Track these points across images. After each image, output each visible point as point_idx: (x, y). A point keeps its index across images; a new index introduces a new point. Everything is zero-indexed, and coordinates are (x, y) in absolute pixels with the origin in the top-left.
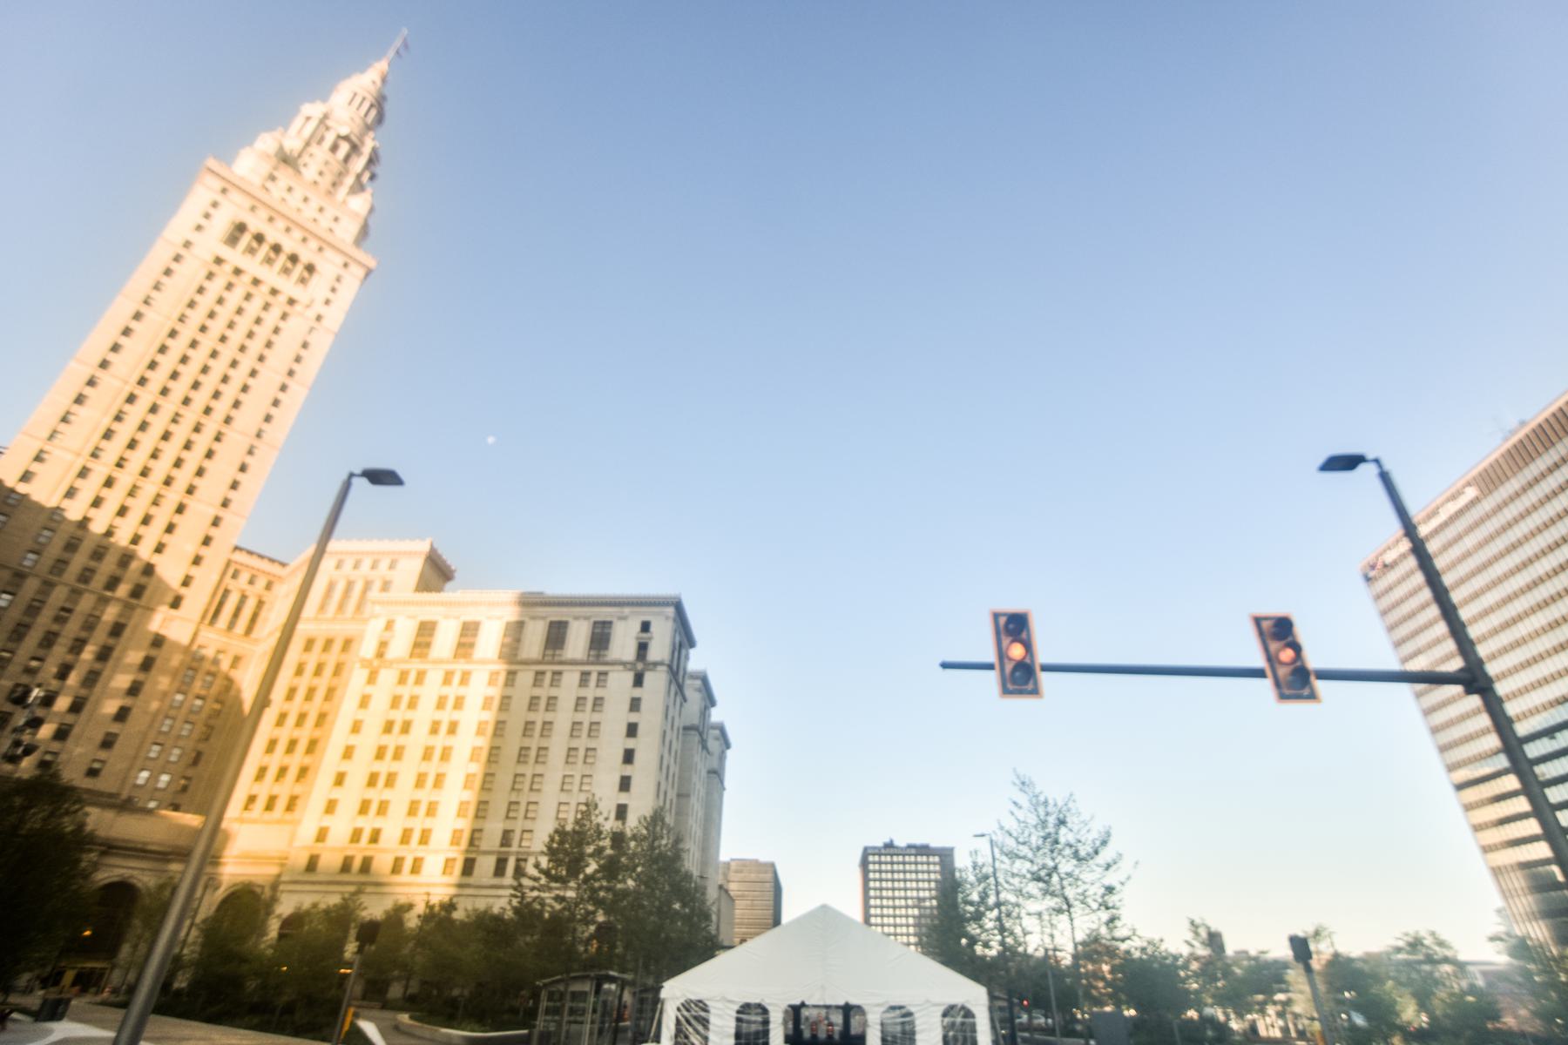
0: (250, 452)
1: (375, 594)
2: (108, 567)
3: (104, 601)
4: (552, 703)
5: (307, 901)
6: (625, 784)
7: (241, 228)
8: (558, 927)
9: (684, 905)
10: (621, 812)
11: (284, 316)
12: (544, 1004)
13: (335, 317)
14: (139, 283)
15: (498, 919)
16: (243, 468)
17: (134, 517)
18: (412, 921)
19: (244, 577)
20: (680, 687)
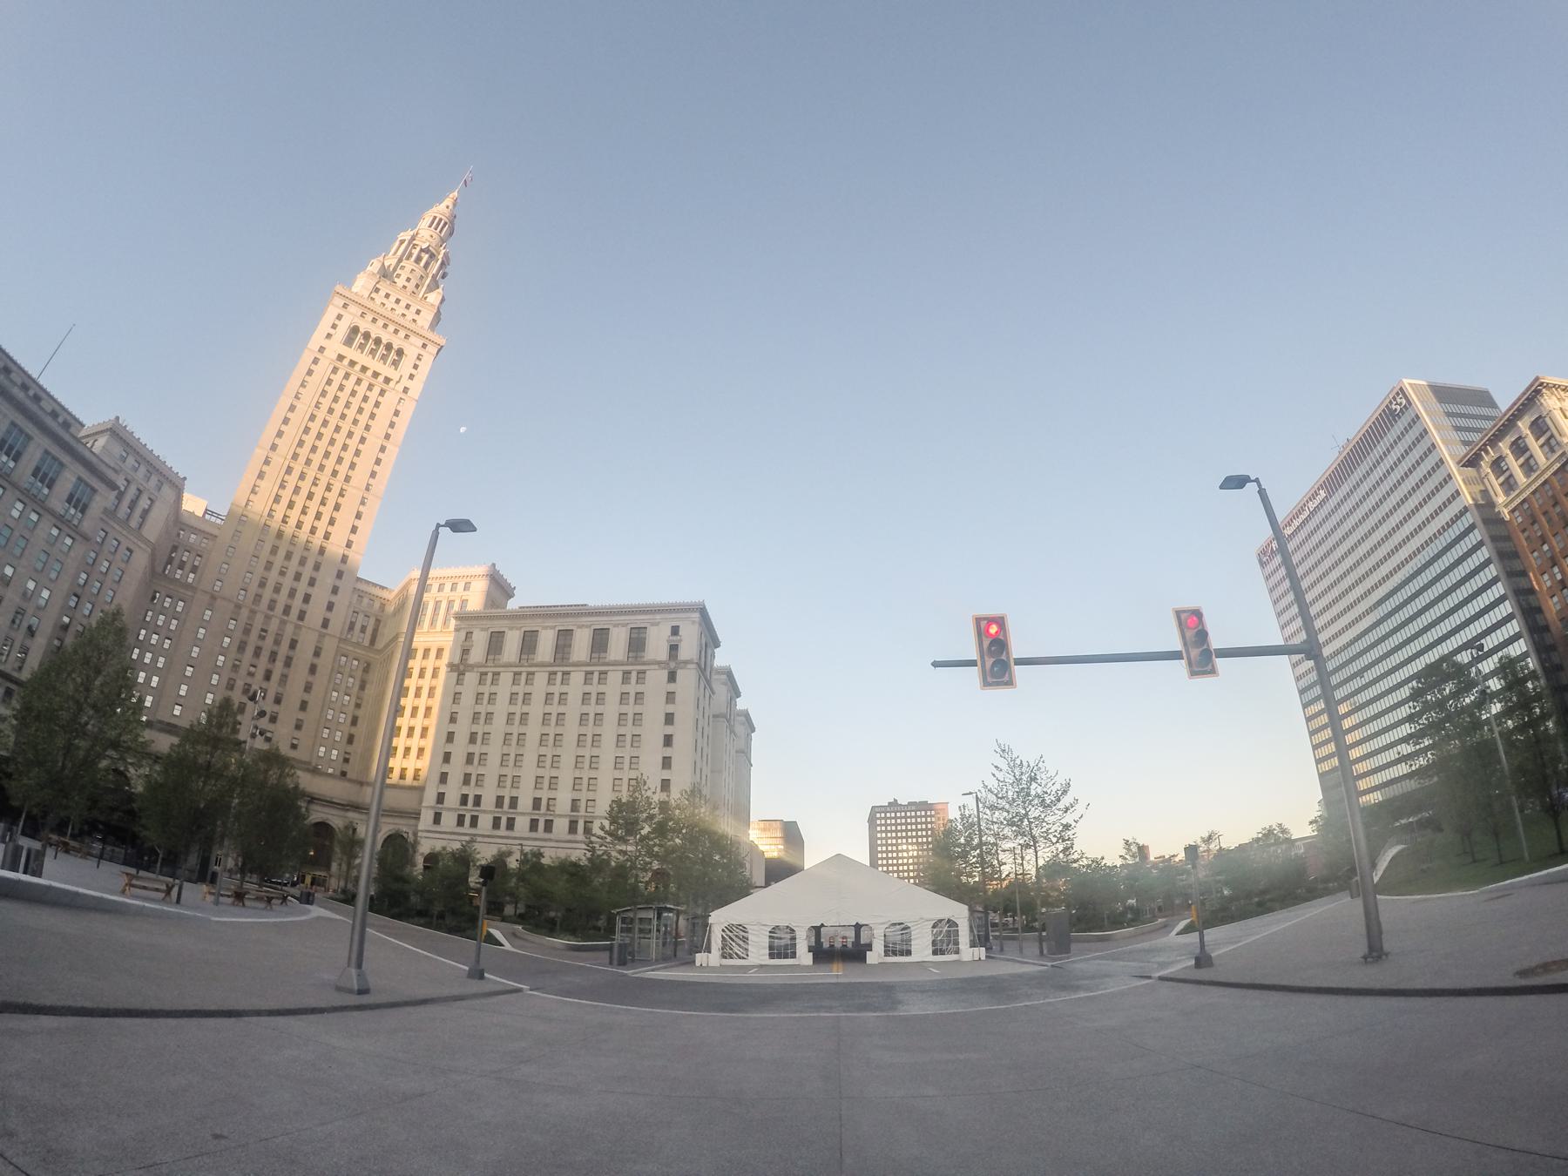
0: (363, 503)
3: (283, 623)
4: (601, 698)
5: (438, 846)
6: (667, 763)
7: (355, 330)
8: (621, 872)
9: (723, 857)
10: (665, 785)
11: (382, 393)
12: (619, 925)
13: (416, 388)
14: (293, 384)
15: (575, 865)
18: (513, 863)
20: (708, 682)
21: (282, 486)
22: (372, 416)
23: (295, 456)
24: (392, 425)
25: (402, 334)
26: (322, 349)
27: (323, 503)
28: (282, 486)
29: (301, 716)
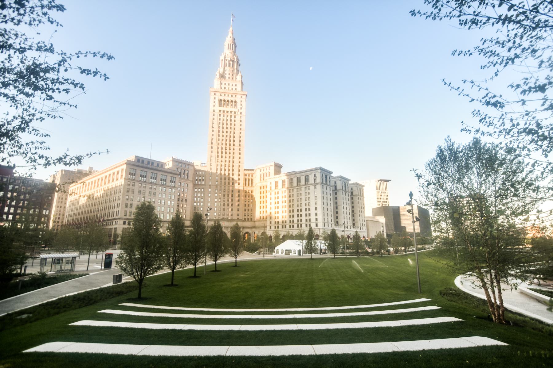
1: (265, 178)
2: (227, 181)
3: (229, 187)
7: (221, 100)
11: (235, 117)
13: (243, 111)
16: (240, 154)
17: (227, 170)
19: (248, 175)
21: (218, 153)
22: (235, 125)
23: (218, 144)
24: (241, 125)
25: (234, 96)
26: (214, 111)
27: (230, 153)
28: (218, 153)
29: (238, 207)
